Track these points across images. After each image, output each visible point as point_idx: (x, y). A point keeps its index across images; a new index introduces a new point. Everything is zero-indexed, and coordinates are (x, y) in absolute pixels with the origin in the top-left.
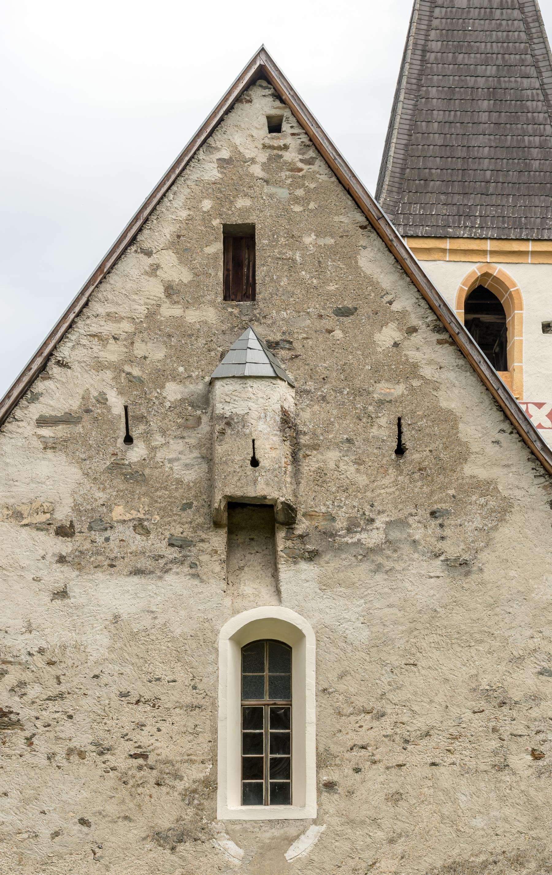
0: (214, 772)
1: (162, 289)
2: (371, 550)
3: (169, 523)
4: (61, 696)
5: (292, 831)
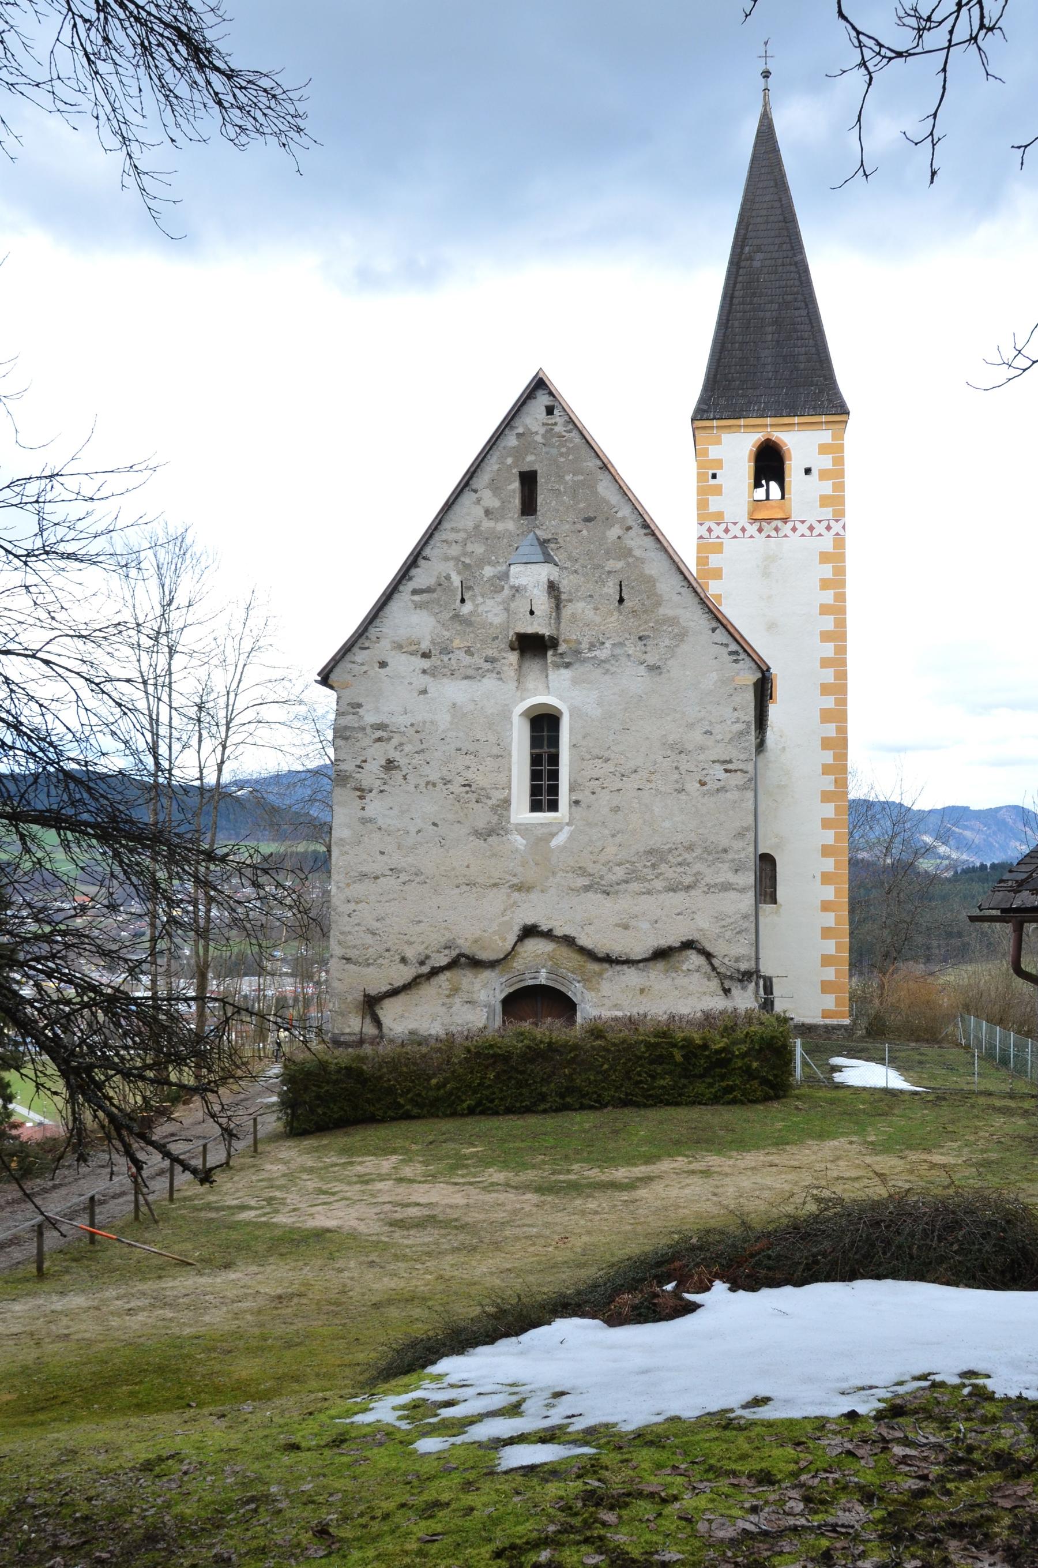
0: (509, 794)
4: (423, 751)
5: (554, 829)
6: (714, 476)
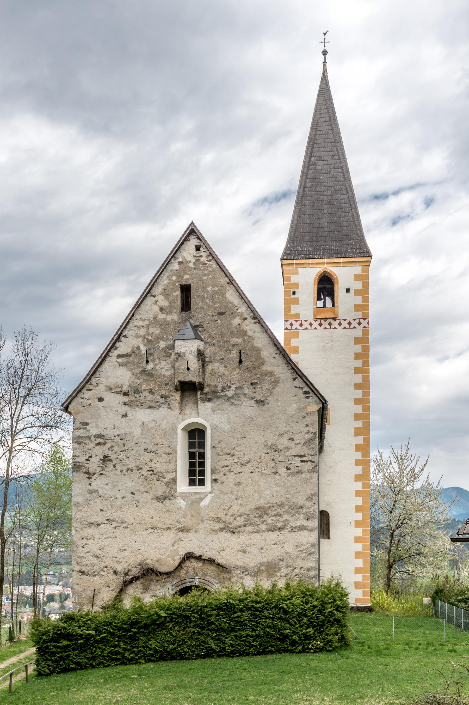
0: (176, 476)
2: (230, 397)
3: (161, 390)
4: (125, 450)
5: (202, 496)
6: (294, 293)
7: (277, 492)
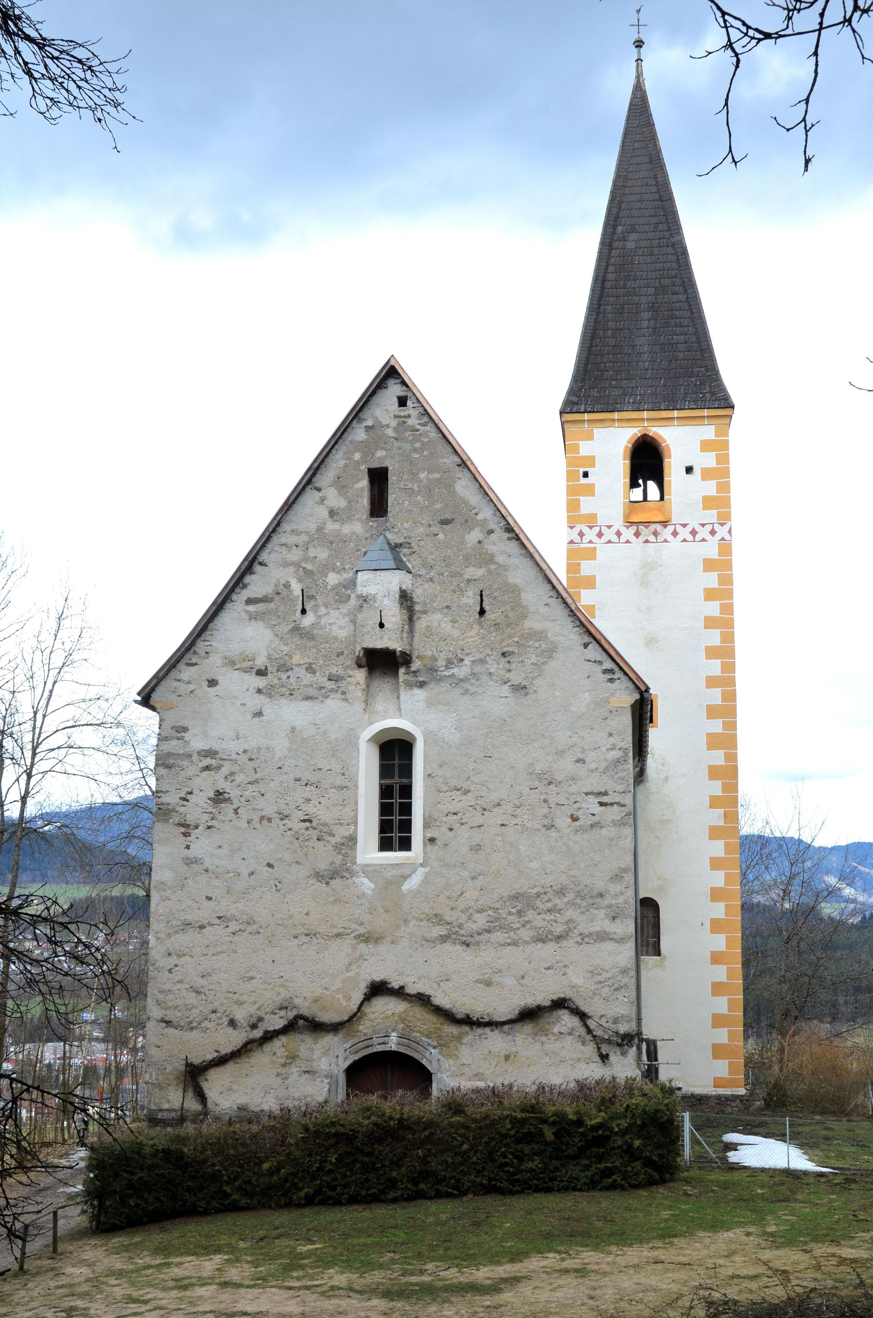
0: (356, 831)
1: (327, 512)
2: (462, 680)
4: (256, 781)
5: (407, 871)
6: (586, 475)
7: (553, 863)
